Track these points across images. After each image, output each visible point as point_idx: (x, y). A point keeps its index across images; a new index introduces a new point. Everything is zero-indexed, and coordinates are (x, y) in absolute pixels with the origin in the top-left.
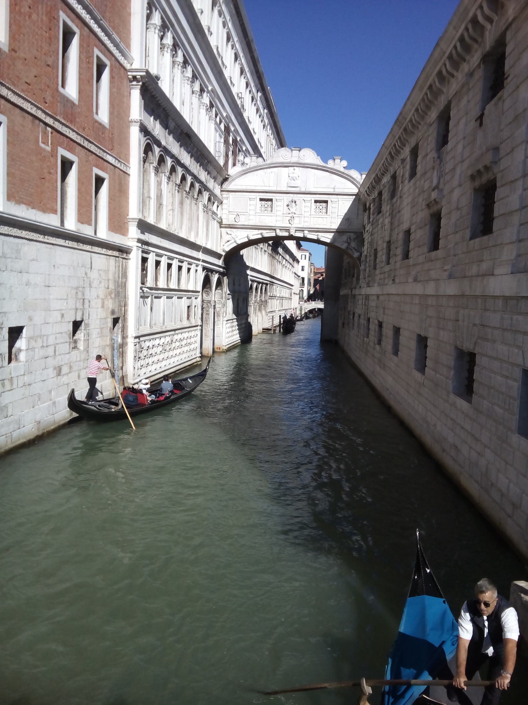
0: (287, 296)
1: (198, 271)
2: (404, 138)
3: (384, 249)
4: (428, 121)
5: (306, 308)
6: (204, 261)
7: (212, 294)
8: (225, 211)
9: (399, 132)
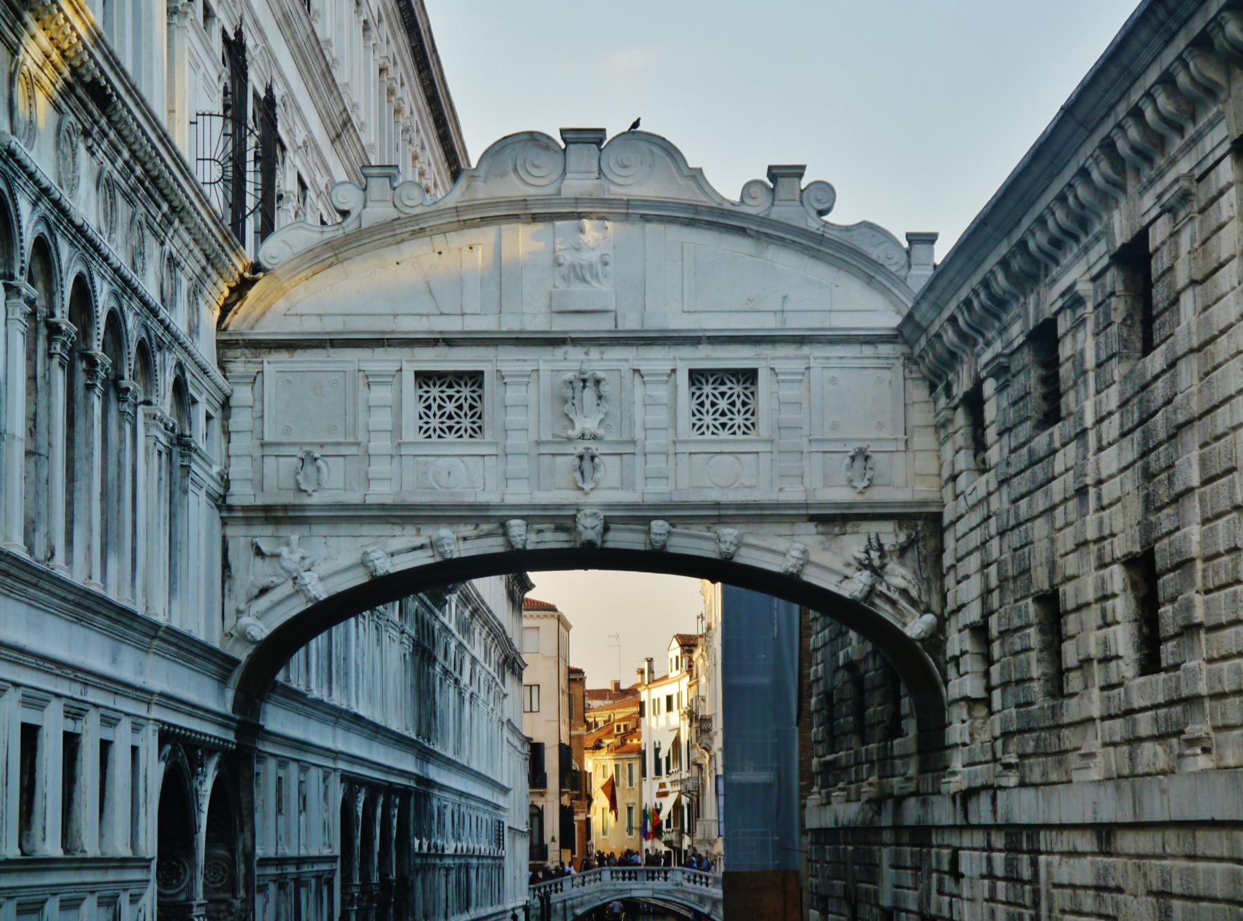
0: (484, 846)
1: (142, 754)
3: (1105, 598)
5: (569, 903)
6: (169, 700)
7: (194, 866)
8: (241, 443)
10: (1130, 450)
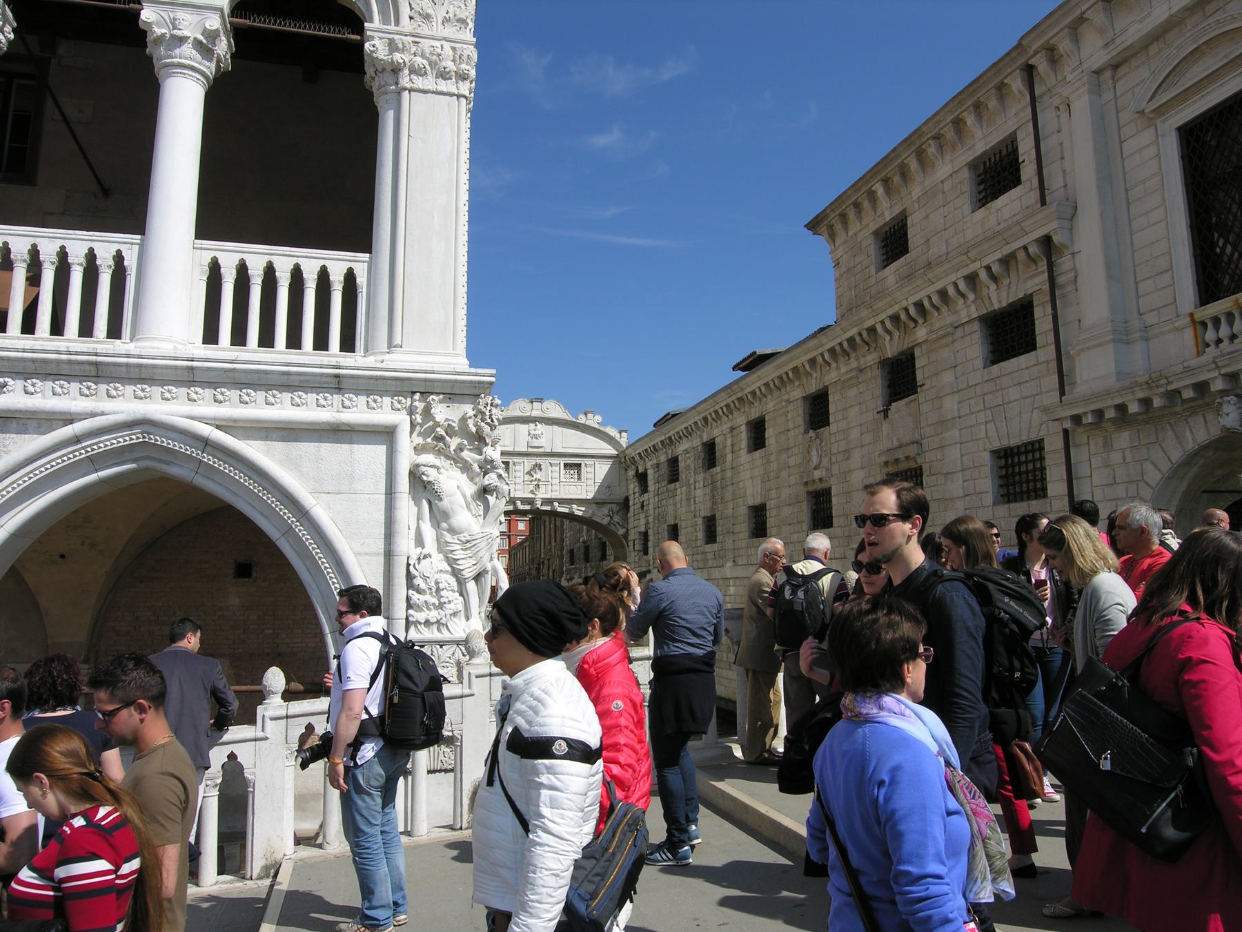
2: (735, 406)
4: (786, 397)
9: (724, 400)
10: (708, 490)
